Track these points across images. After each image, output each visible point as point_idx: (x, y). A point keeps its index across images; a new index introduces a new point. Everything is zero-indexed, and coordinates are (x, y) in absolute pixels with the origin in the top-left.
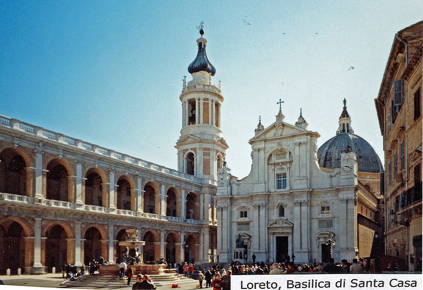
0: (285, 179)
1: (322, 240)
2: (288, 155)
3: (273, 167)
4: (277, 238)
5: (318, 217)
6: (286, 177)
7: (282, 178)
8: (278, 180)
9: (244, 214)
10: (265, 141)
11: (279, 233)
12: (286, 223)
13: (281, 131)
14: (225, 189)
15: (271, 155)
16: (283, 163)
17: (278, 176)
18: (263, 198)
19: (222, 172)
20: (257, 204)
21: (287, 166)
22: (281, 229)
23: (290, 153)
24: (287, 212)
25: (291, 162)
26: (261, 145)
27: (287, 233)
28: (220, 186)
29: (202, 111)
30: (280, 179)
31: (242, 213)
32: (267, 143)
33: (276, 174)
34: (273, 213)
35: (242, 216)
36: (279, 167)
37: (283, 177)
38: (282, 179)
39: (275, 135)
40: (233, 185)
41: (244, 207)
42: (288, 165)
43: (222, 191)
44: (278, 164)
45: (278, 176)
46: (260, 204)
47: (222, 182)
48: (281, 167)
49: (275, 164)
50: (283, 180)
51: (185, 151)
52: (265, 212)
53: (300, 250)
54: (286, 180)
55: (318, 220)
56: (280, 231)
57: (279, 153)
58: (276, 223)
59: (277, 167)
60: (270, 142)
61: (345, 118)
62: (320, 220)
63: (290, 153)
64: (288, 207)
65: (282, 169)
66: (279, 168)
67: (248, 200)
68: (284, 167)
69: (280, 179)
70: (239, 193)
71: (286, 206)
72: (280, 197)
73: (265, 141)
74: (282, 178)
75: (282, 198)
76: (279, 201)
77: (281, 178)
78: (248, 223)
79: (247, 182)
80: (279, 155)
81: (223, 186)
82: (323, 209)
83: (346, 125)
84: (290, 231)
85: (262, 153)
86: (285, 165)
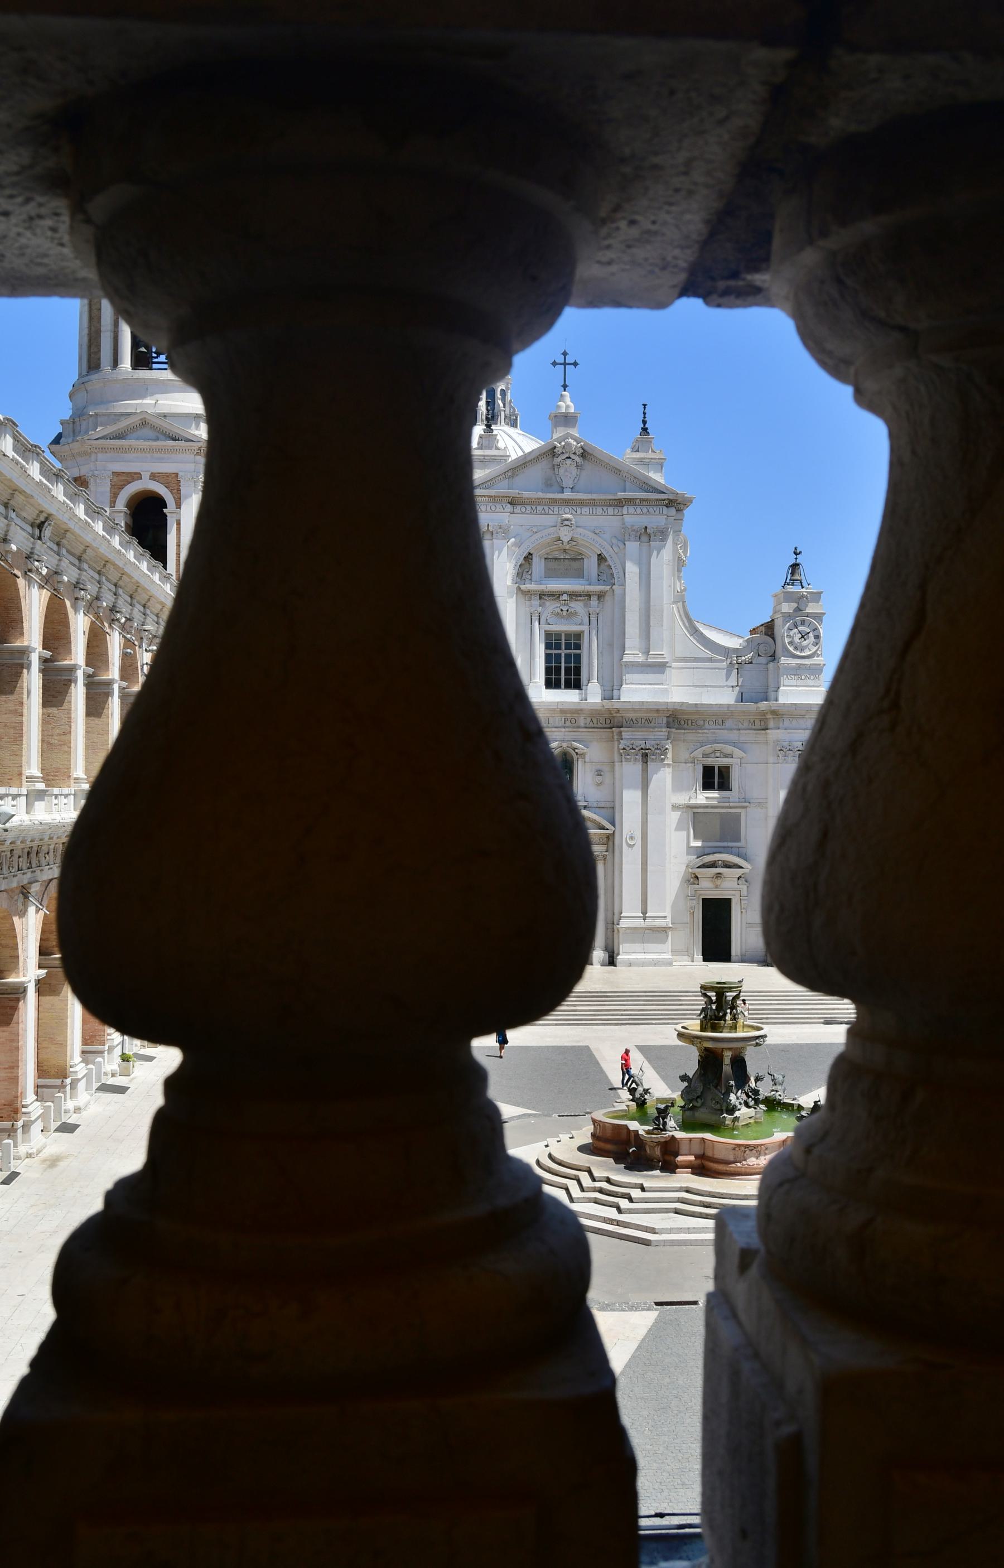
0: (577, 652)
2: (591, 565)
6: (578, 647)
7: (563, 646)
13: (574, 471)
15: (528, 558)
16: (574, 595)
21: (586, 605)
23: (601, 558)
30: (554, 652)
32: (518, 509)
37: (568, 646)
38: (563, 652)
42: (594, 602)
44: (556, 596)
48: (565, 609)
49: (542, 595)
51: (122, 479)
53: (640, 923)
54: (578, 658)
57: (557, 554)
59: (551, 606)
60: (528, 507)
63: (601, 558)
64: (587, 760)
65: (571, 615)
69: (554, 652)
71: (583, 755)
74: (563, 646)
77: (558, 647)
80: (556, 559)
86: (581, 604)
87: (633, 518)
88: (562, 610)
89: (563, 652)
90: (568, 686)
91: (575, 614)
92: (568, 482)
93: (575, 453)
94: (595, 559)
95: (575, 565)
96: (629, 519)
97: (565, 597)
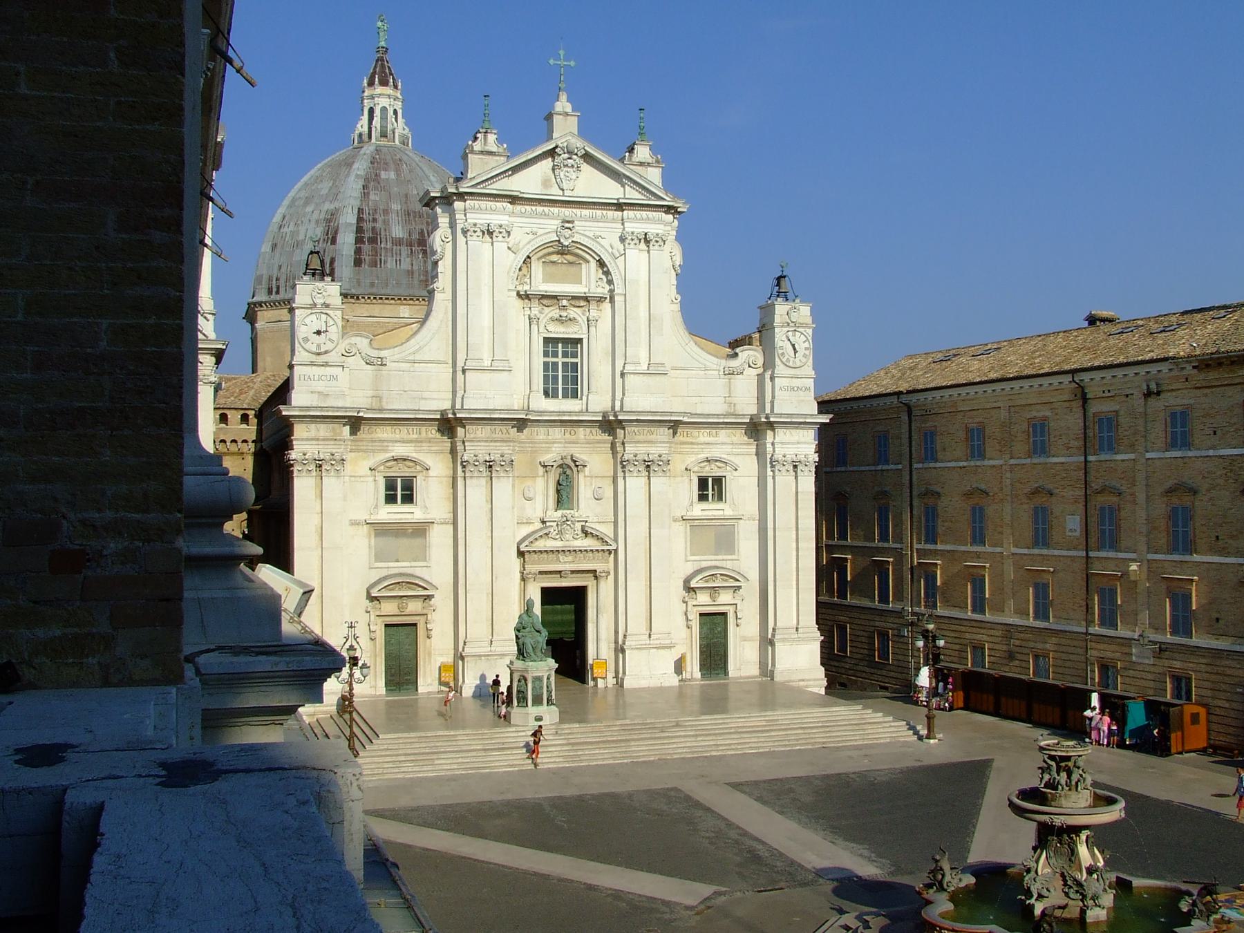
1: (703, 598)
3: (535, 311)
5: (689, 515)
8: (546, 364)
10: (514, 199)
14: (334, 378)
17: (550, 343)
18: (505, 431)
19: (319, 301)
22: (570, 558)
23: (601, 264)
24: (584, 488)
26: (498, 214)
28: (312, 364)
31: (390, 485)
32: (518, 208)
33: (544, 338)
34: (531, 495)
35: (391, 499)
36: (555, 312)
37: (565, 355)
38: (560, 360)
39: (546, 183)
40: (354, 362)
43: (320, 386)
45: (550, 343)
46: (496, 457)
47: (318, 346)
50: (565, 365)
52: (513, 486)
55: (688, 525)
56: (566, 564)
60: (528, 208)
61: (388, 90)
62: (696, 523)
63: (601, 264)
64: (587, 473)
66: (557, 316)
67: (424, 434)
68: (576, 316)
70: (380, 398)
72: (557, 433)
73: (514, 199)
75: (567, 435)
77: (555, 355)
78: (420, 530)
79: (418, 357)
80: (552, 262)
81: (326, 365)
83: (391, 112)
85: (500, 246)
87: (637, 223)
88: (561, 316)
89: (560, 360)
90: (565, 396)
91: (575, 319)
93: (576, 154)
94: (593, 264)
95: (572, 269)
96: (630, 227)
97: (565, 302)
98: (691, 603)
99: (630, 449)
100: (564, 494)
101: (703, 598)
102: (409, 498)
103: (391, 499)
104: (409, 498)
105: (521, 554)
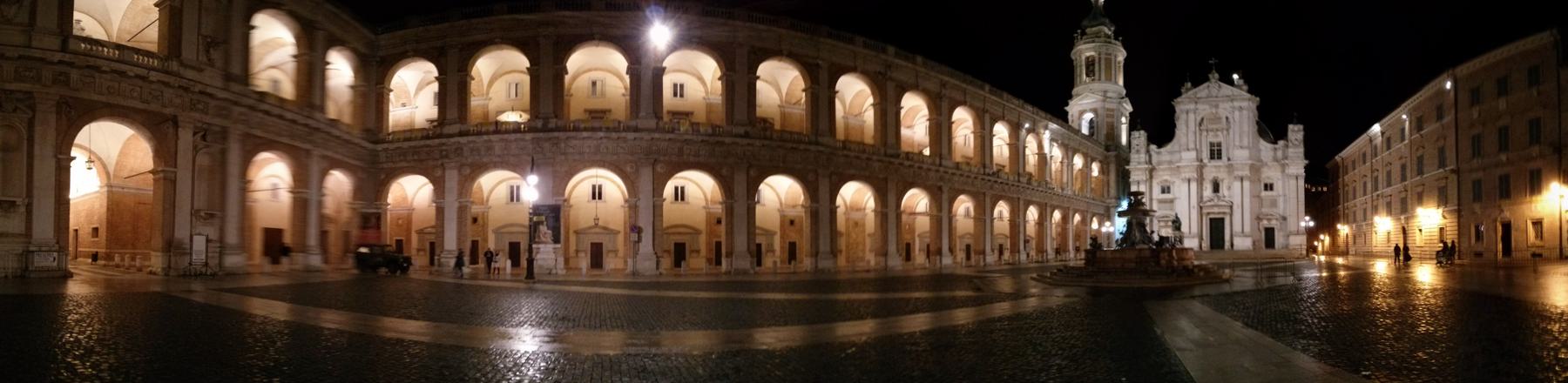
1: (1265, 222)
4: (1211, 219)
8: (1211, 150)
9: (1166, 190)
11: (1213, 213)
12: (1223, 201)
15: (1202, 119)
20: (1187, 177)
23: (1227, 118)
25: (1227, 130)
27: (1224, 213)
29: (1103, 67)
35: (1163, 192)
38: (1216, 148)
41: (1166, 181)
42: (1225, 132)
45: (1212, 145)
46: (1191, 177)
54: (1220, 150)
58: (1209, 201)
59: (1211, 134)
63: (1227, 118)
72: (1214, 170)
76: (1214, 175)
78: (1172, 201)
82: (1266, 186)
84: (1228, 210)
92: (1214, 94)
98: (1261, 223)
99: (1236, 173)
100: (1216, 188)
101: (1265, 222)
102: (1169, 192)
103: (1163, 192)
104: (1169, 192)
105: (1201, 208)
